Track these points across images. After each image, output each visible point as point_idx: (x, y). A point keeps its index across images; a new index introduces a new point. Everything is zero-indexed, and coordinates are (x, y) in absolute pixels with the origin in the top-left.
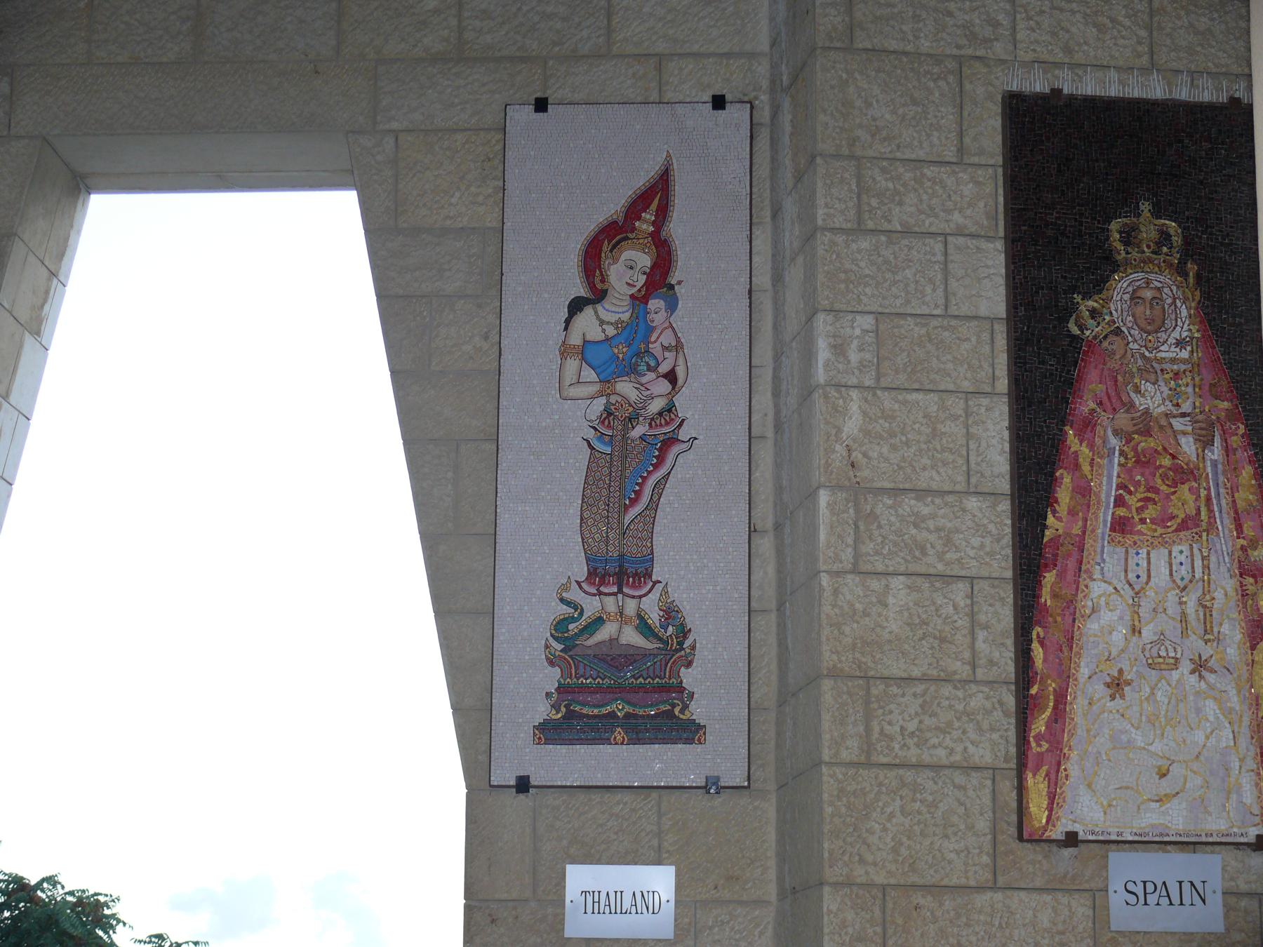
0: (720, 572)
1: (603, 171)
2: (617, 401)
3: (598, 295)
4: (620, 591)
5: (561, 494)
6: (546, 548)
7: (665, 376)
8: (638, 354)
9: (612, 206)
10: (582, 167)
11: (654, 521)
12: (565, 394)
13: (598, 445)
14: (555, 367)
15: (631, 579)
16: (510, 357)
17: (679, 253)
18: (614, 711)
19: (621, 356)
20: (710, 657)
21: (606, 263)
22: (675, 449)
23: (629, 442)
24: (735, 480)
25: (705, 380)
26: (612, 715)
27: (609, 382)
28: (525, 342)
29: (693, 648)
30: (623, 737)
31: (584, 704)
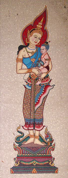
0: (62, 123)
1: (27, 11)
2: (32, 74)
3: (27, 45)
4: (34, 129)
5: (17, 101)
6: (13, 116)
7: (46, 67)
8: (39, 61)
9: (30, 21)
10: (21, 9)
11: (43, 109)
12: (18, 72)
13: (27, 87)
14: (15, 65)
15: (37, 125)
16: (2, 62)
17: (49, 33)
18: (33, 163)
19: (33, 62)
20: (59, 148)
21: (29, 36)
22: (49, 88)
23: (36, 86)
24: (66, 97)
25: (57, 69)
26: (32, 165)
27: (30, 69)
28: (6, 58)
29: (54, 145)
30: (35, 171)
31: (24, 162)
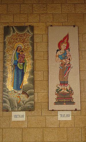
8: (65, 57)
9: (62, 39)
22: (70, 68)
